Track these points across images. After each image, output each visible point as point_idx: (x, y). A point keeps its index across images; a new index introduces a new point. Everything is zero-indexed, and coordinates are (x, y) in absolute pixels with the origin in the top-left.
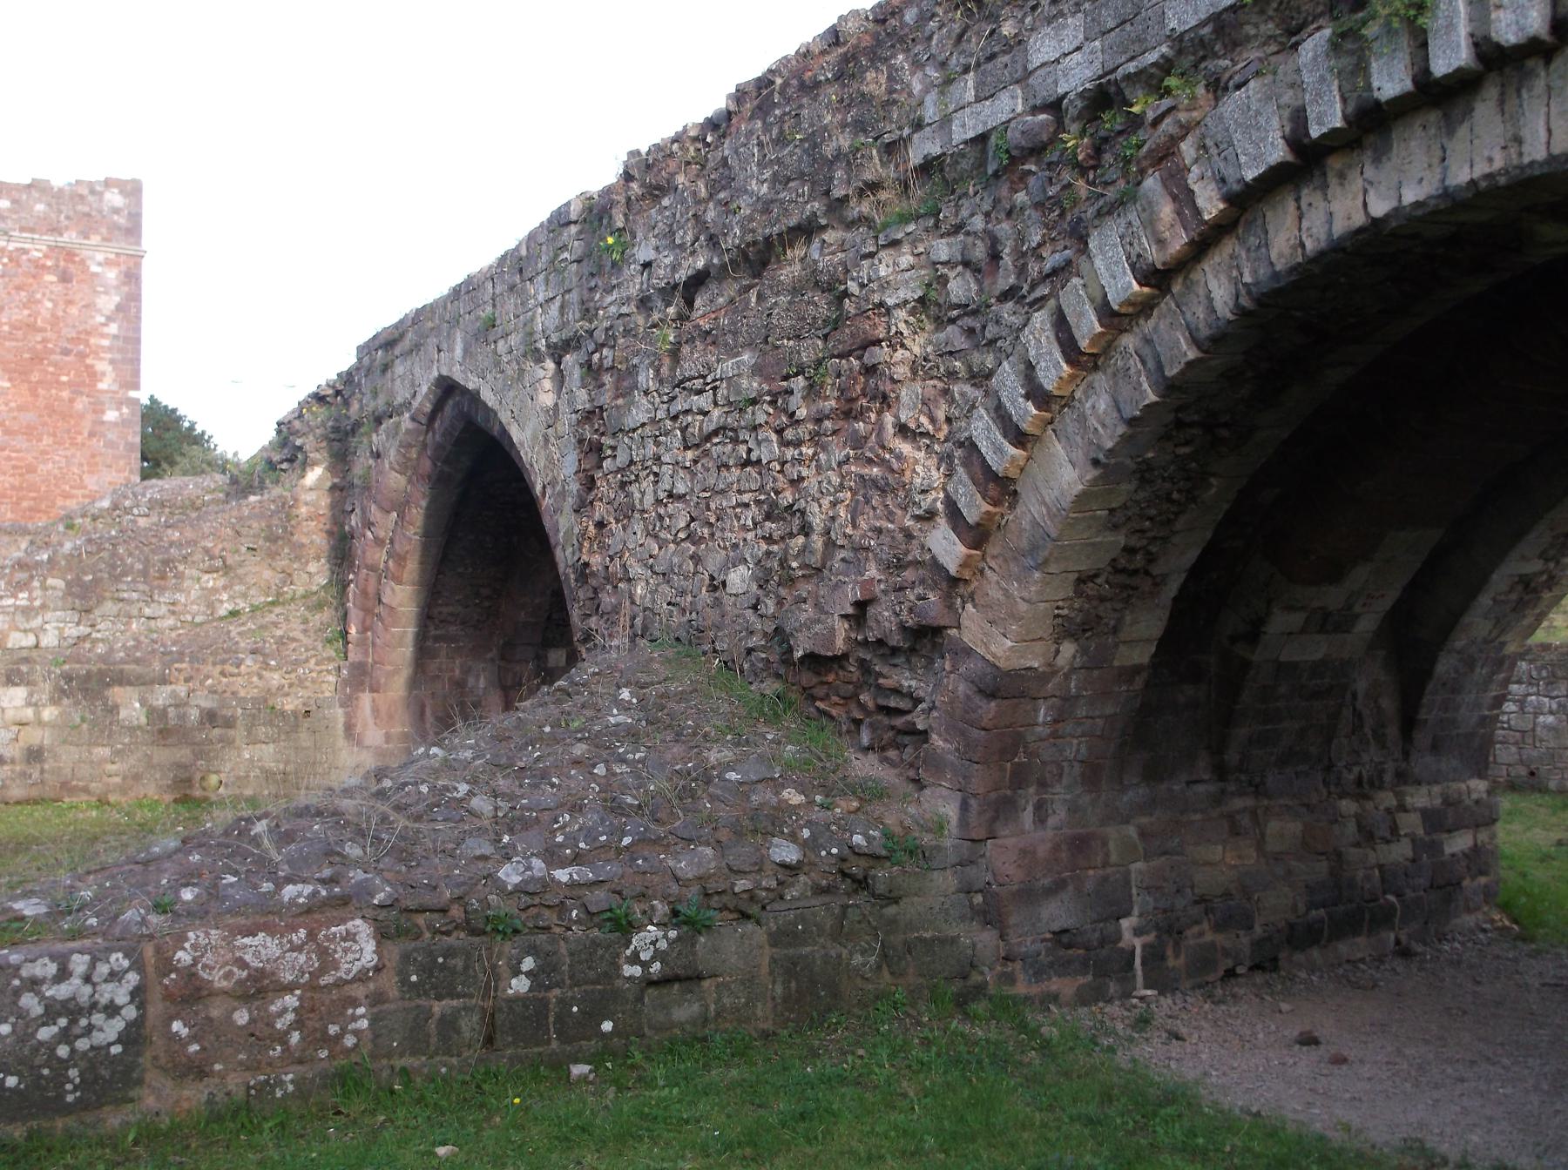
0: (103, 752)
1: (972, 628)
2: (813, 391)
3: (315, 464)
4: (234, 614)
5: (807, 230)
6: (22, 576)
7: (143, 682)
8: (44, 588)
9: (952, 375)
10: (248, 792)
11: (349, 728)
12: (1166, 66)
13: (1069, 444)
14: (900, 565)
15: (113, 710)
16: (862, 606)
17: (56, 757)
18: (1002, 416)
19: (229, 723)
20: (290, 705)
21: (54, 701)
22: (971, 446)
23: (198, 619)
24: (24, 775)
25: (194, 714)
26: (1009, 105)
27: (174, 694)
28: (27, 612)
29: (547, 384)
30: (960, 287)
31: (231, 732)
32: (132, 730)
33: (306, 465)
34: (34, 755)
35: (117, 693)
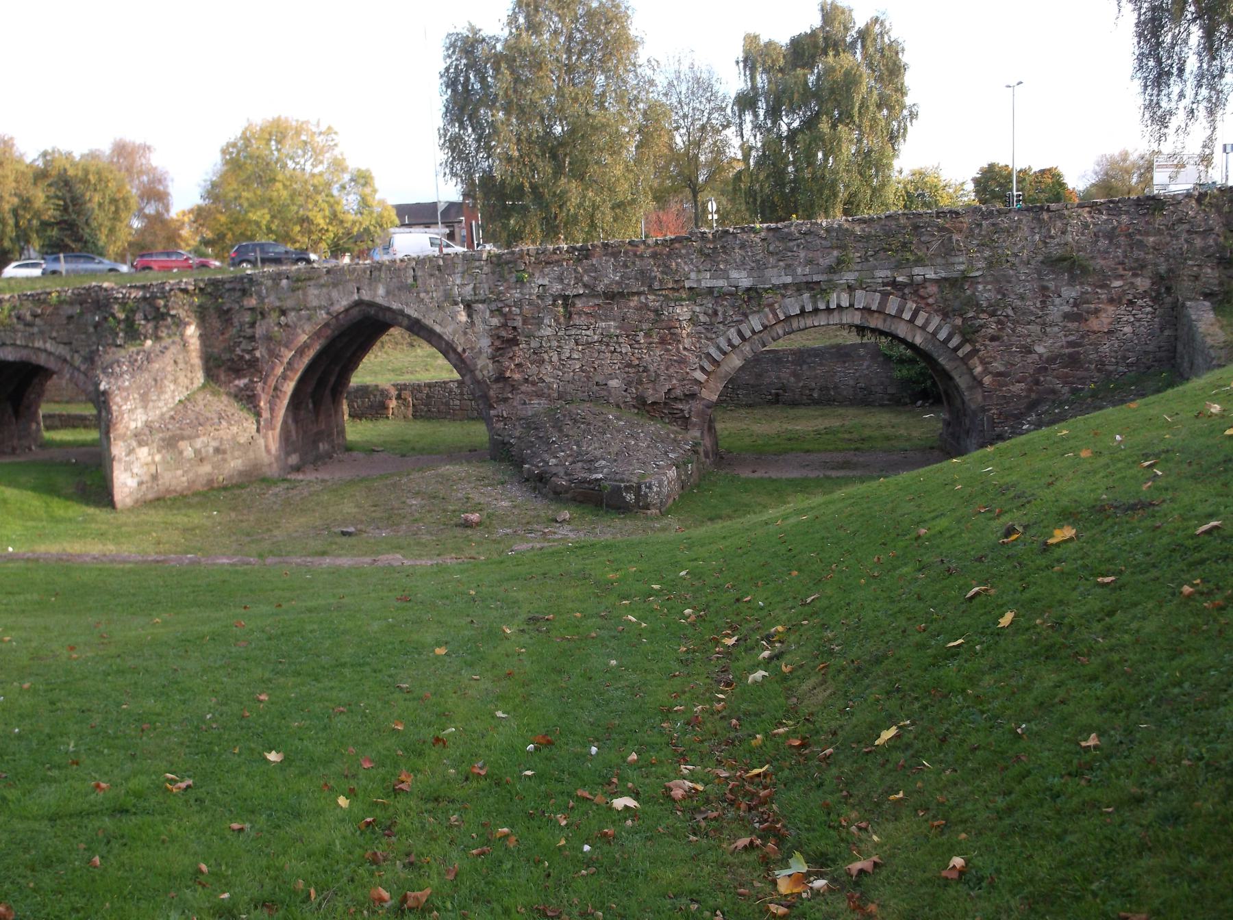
0: (180, 472)
1: (705, 393)
2: (648, 335)
3: (188, 324)
4: (180, 401)
5: (639, 294)
6: (125, 394)
7: (190, 438)
8: (134, 399)
9: (701, 338)
10: (234, 482)
11: (266, 446)
12: (770, 288)
13: (737, 355)
14: (684, 380)
15: (181, 453)
16: (669, 390)
17: (163, 478)
18: (719, 348)
19: (224, 452)
20: (242, 440)
21: (159, 451)
22: (708, 355)
23: (172, 406)
24: (152, 487)
25: (211, 450)
26: (721, 283)
27: (203, 442)
28: (131, 411)
29: (463, 313)
30: (702, 318)
31: (226, 456)
32: (189, 460)
33: (180, 324)
34: (155, 477)
35: (182, 444)
